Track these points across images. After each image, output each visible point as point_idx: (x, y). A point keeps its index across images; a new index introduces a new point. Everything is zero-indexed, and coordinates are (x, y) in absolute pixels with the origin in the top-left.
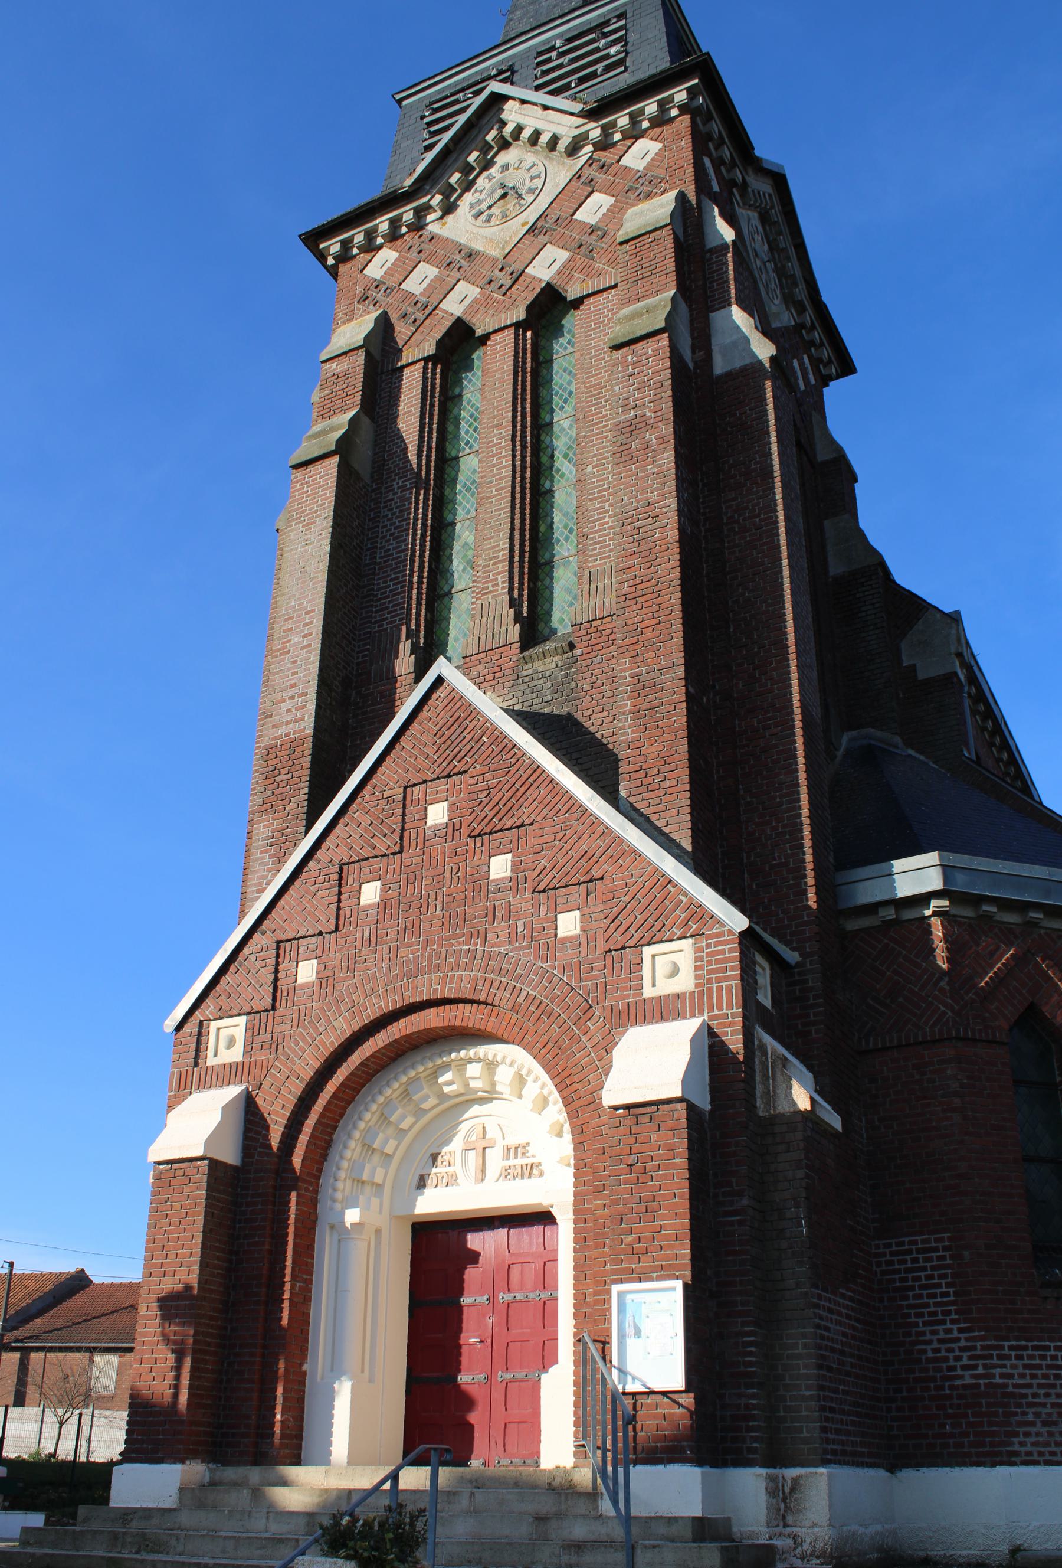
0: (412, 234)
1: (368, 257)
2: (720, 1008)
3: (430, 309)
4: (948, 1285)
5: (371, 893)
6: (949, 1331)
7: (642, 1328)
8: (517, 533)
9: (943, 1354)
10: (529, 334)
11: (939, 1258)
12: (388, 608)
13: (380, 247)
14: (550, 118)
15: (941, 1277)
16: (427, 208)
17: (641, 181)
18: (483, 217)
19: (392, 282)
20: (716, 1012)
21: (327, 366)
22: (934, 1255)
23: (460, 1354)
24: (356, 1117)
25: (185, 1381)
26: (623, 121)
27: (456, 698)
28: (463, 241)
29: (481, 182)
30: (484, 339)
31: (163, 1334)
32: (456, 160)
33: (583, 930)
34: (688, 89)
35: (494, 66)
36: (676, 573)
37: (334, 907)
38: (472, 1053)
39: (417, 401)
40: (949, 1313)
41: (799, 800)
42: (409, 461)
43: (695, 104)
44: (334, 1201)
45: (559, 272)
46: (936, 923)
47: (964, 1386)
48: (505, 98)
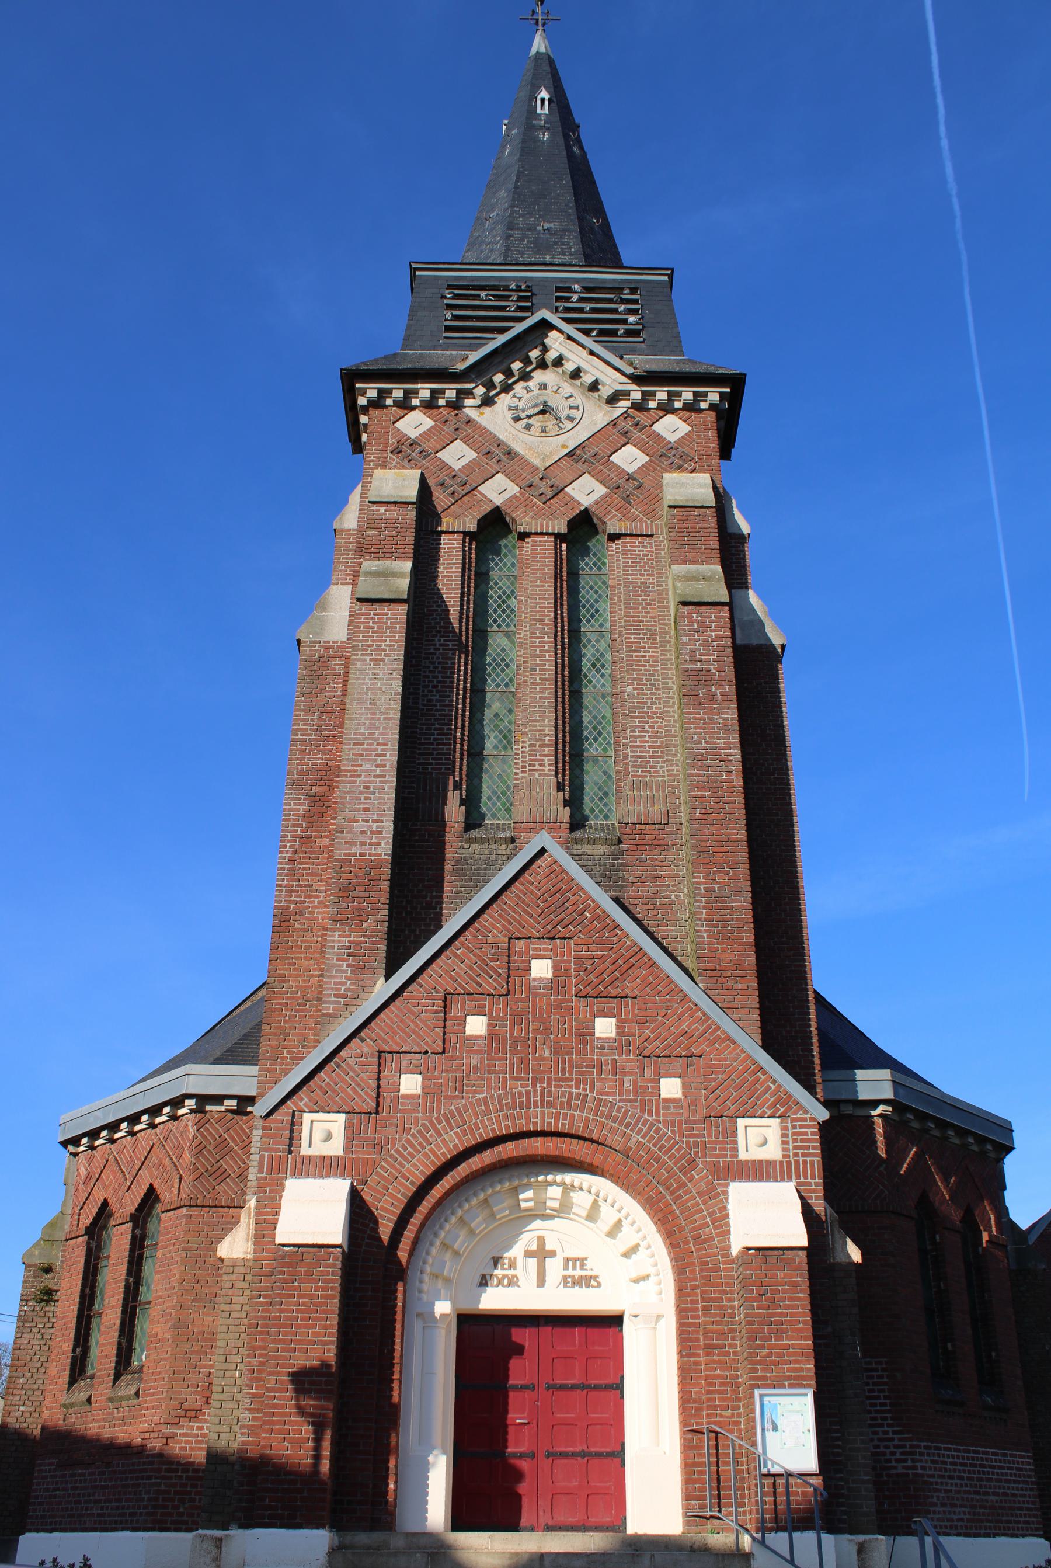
0: (448, 410)
1: (401, 412)
2: (806, 1177)
3: (468, 488)
4: (885, 1397)
5: (476, 1025)
6: (886, 1432)
7: (778, 1423)
8: (560, 723)
9: (882, 1449)
10: (564, 546)
11: (879, 1377)
12: (432, 754)
13: (414, 408)
14: (594, 364)
15: (880, 1391)
16: (469, 393)
17: (674, 452)
18: (523, 423)
19: (429, 446)
20: (802, 1180)
21: (375, 507)
22: (875, 1374)
23: (506, 1433)
24: (442, 1220)
25: (326, 1452)
26: (662, 395)
27: (557, 871)
28: (502, 437)
29: (519, 388)
30: (523, 536)
31: (299, 1407)
32: (501, 362)
33: (684, 1094)
34: (720, 393)
35: (514, 279)
36: (741, 814)
37: (440, 1031)
39: (457, 568)
40: (886, 1419)
41: (809, 1014)
42: (451, 623)
43: (721, 407)
44: (420, 1291)
45: (597, 503)
46: (879, 1122)
47: (897, 1474)
48: (552, 327)
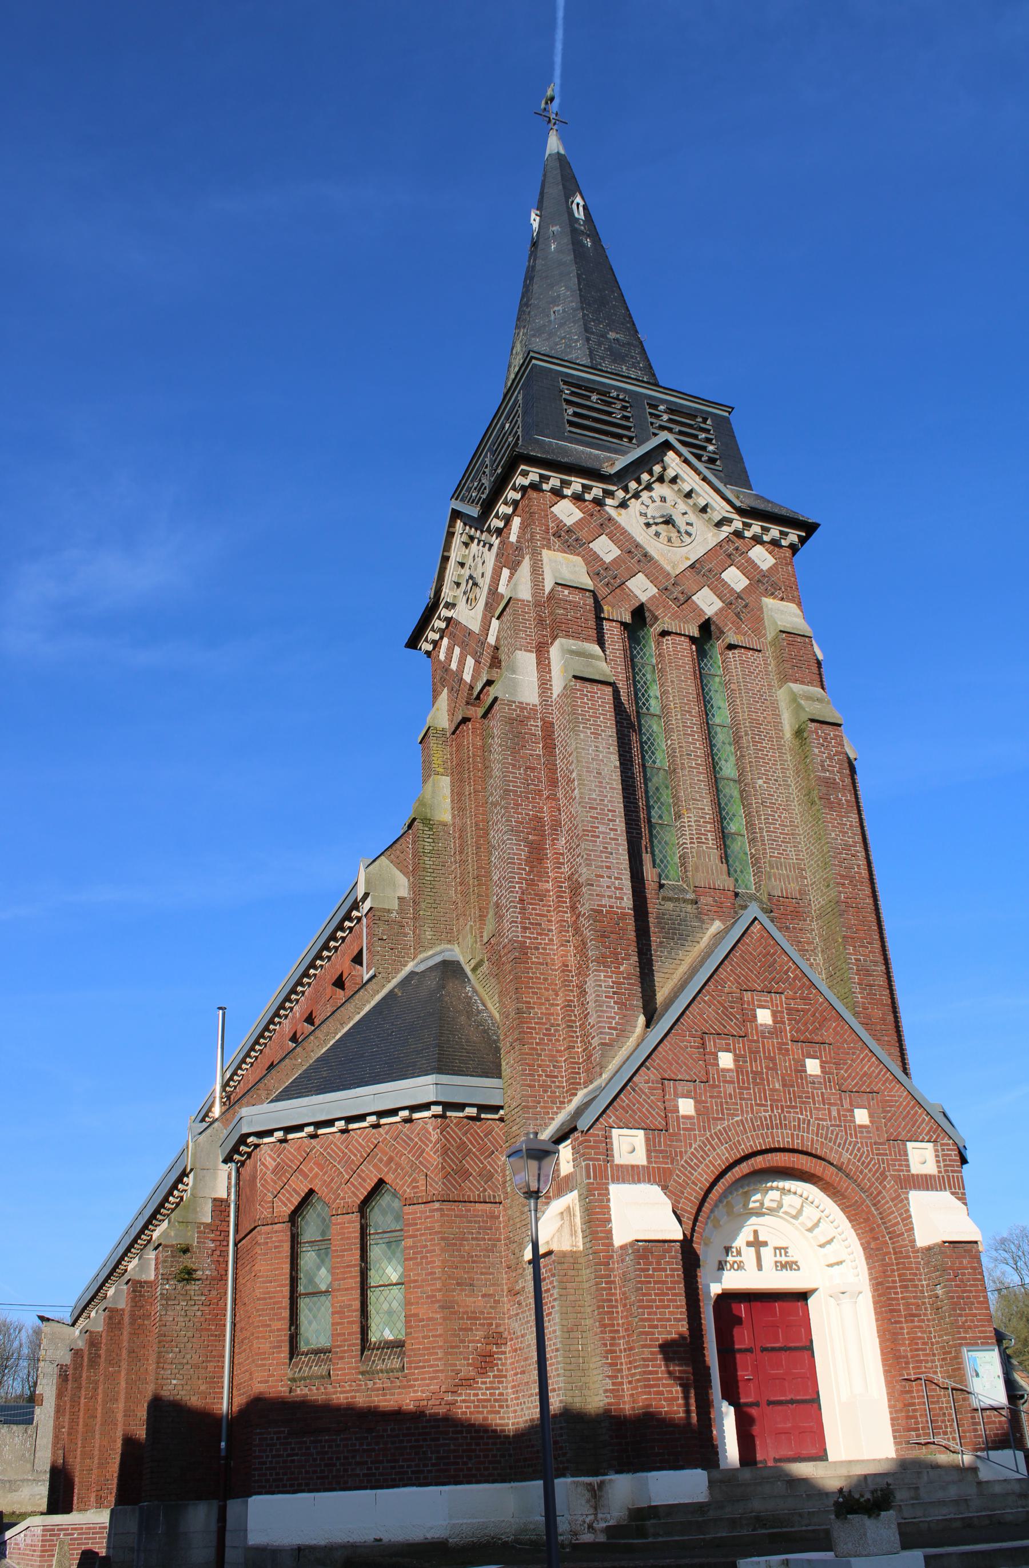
1: (555, 498)
13: (564, 497)
19: (582, 534)
23: (738, 1387)
26: (756, 528)
31: (669, 1372)
34: (799, 536)
38: (775, 1184)
45: (716, 614)
